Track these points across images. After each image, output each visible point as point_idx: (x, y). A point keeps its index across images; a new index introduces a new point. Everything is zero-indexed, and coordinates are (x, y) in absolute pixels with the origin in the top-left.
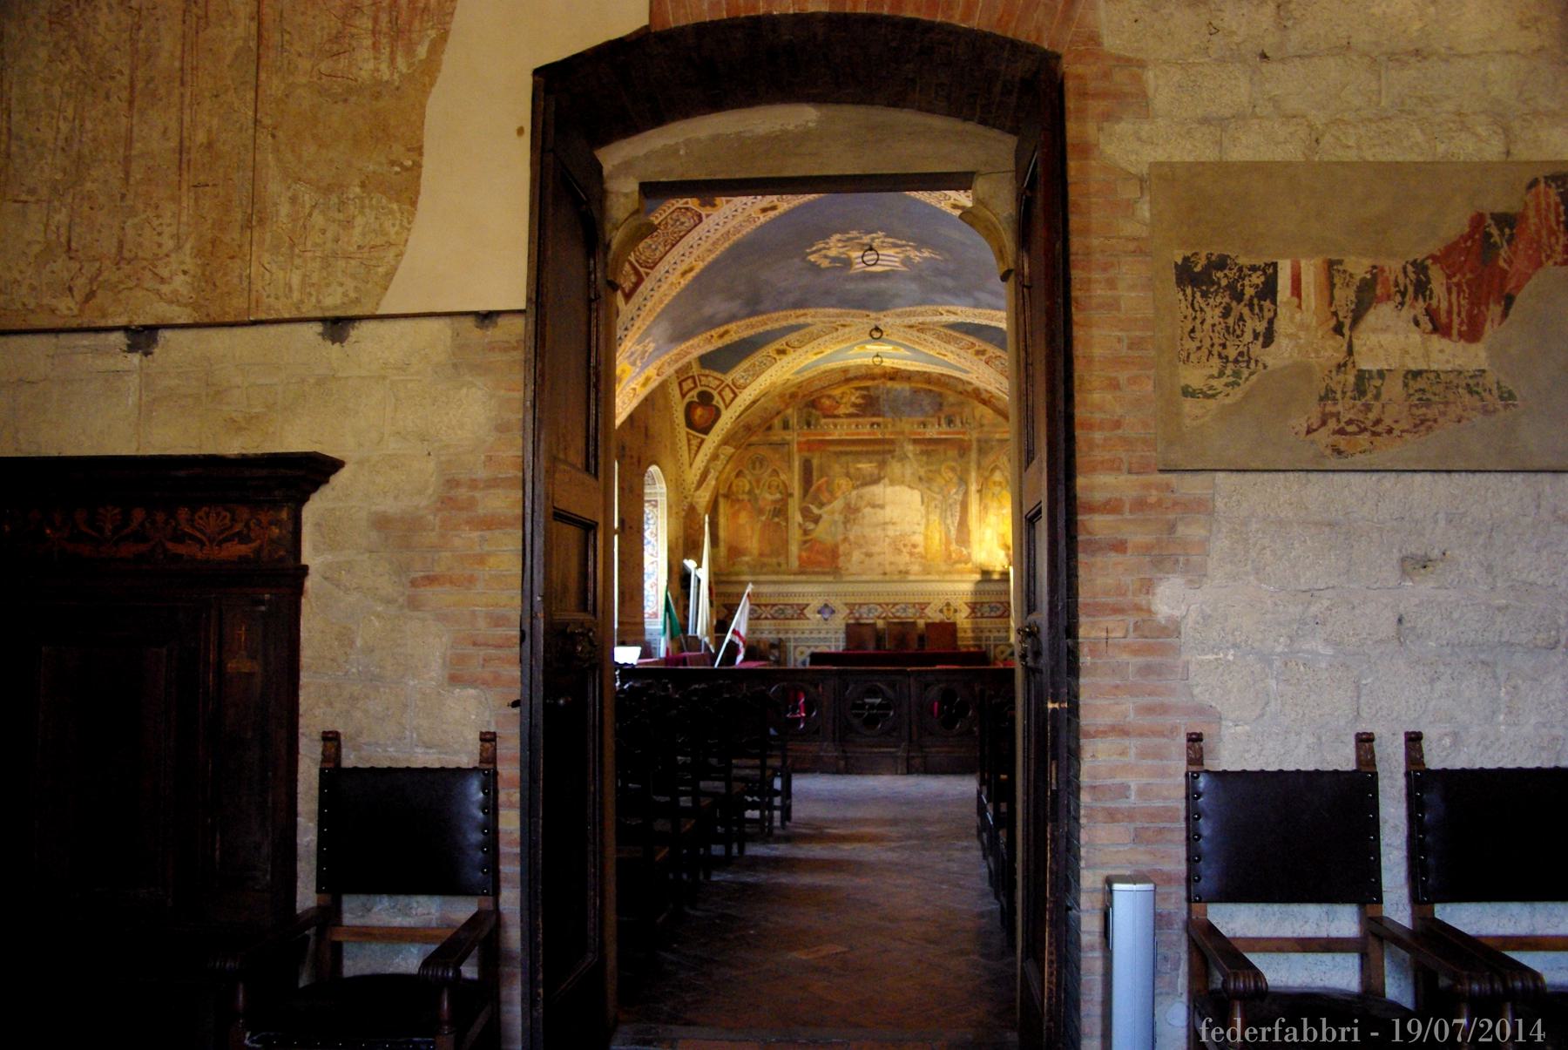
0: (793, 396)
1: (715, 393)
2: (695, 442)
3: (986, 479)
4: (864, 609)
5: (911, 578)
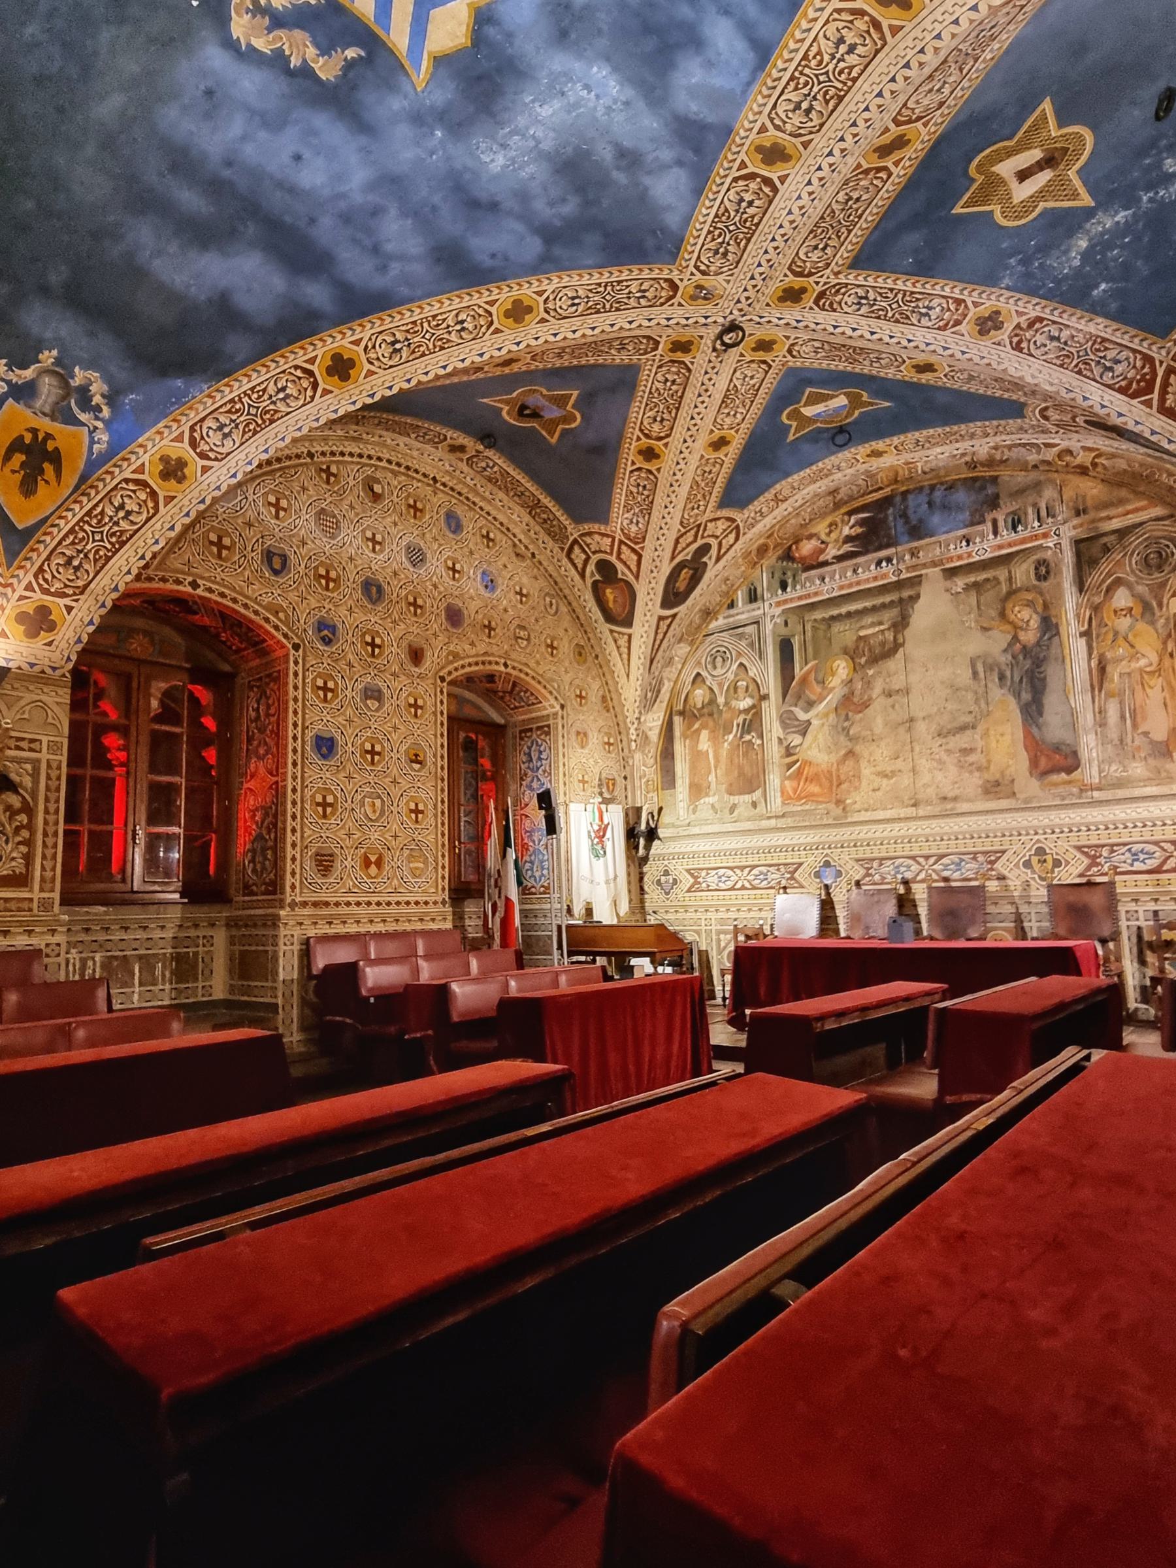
0: (762, 551)
1: (613, 559)
2: (623, 642)
3: (1096, 609)
4: (888, 868)
5: (964, 807)
